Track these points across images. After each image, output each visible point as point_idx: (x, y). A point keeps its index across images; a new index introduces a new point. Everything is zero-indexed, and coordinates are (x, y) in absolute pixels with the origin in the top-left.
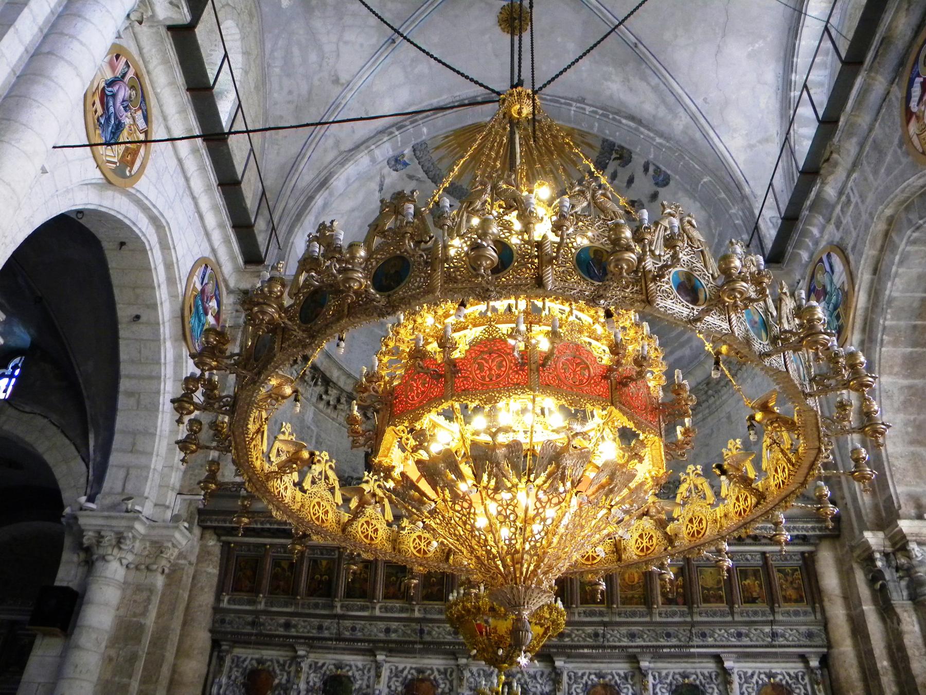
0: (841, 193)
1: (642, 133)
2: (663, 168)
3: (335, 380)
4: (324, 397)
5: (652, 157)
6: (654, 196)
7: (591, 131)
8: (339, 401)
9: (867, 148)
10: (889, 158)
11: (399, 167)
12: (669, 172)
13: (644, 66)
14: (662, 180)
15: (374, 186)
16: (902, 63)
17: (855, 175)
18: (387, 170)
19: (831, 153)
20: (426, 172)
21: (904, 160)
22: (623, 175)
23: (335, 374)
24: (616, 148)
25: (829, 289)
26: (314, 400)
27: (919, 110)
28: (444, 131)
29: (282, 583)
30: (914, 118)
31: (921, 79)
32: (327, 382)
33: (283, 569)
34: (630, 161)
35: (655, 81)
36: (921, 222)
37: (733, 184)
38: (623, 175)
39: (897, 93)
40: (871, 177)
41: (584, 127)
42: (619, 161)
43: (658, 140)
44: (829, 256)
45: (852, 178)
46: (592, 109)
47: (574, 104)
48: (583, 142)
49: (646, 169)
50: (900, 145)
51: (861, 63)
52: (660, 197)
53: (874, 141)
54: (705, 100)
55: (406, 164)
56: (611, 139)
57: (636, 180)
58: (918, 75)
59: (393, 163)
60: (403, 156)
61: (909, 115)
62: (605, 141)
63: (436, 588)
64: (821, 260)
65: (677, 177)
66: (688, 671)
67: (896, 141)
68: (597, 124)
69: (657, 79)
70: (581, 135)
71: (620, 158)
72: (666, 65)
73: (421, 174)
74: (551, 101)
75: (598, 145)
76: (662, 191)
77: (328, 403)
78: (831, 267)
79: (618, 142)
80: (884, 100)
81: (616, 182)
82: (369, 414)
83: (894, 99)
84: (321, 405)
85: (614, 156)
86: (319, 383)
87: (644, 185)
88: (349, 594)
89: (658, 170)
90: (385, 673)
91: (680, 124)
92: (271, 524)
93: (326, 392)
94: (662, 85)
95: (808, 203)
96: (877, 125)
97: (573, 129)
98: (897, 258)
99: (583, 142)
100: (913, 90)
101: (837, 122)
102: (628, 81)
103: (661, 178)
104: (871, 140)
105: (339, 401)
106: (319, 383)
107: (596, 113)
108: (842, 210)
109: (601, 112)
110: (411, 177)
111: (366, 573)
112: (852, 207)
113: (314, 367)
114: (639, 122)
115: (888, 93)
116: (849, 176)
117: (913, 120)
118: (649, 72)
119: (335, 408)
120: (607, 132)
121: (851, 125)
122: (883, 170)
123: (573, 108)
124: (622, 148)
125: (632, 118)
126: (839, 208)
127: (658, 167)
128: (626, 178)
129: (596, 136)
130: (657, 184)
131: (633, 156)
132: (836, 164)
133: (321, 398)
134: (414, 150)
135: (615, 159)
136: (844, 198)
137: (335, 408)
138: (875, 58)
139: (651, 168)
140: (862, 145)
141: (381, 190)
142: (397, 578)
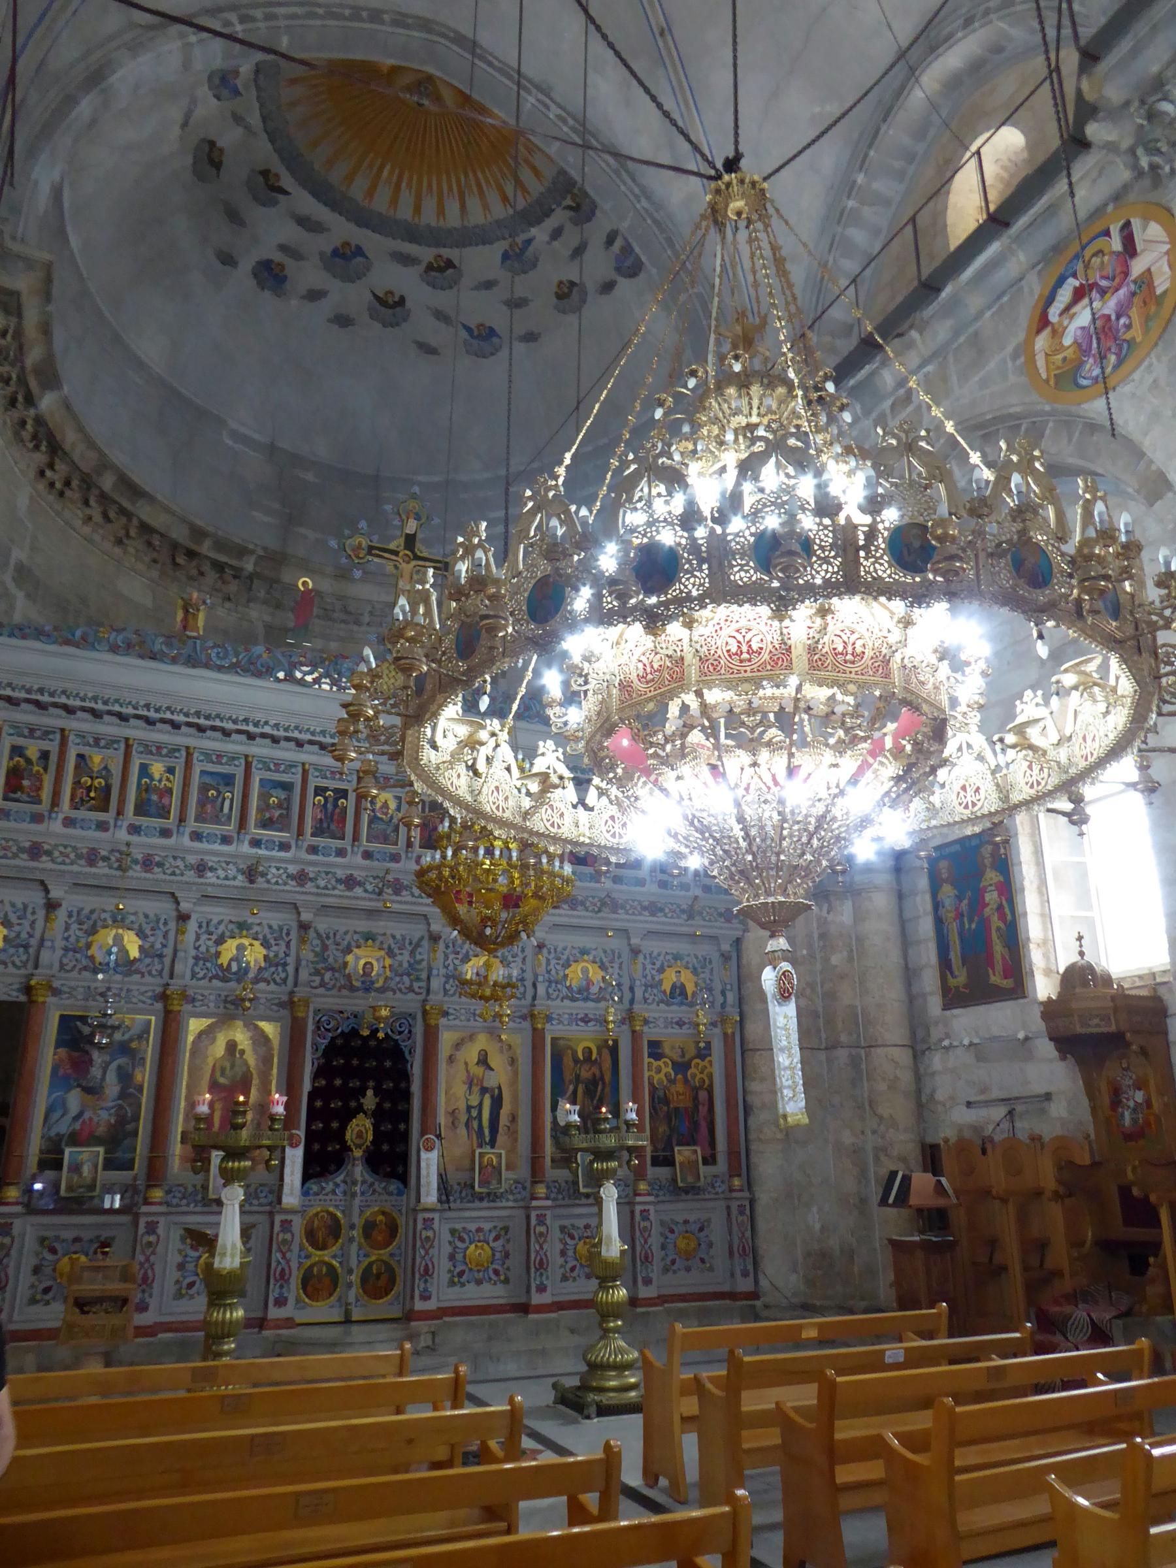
1: (625, 184)
2: (637, 249)
3: (67, 447)
4: (48, 473)
6: (608, 287)
7: (547, 150)
8: (67, 483)
9: (962, 339)
10: (992, 365)
11: (225, 93)
12: (643, 259)
14: (630, 266)
15: (175, 113)
16: (1057, 249)
17: (929, 368)
18: (204, 91)
19: (911, 327)
20: (264, 119)
21: (1012, 379)
22: (571, 237)
23: (70, 438)
24: (576, 191)
26: (32, 474)
27: (1060, 323)
29: (26, 783)
30: (1048, 330)
31: (1077, 283)
32: (55, 449)
33: (29, 761)
34: (589, 220)
38: (571, 237)
39: (1035, 287)
40: (954, 379)
42: (572, 213)
43: (644, 203)
45: (925, 370)
46: (559, 112)
47: (534, 91)
48: (526, 161)
49: (610, 240)
50: (1015, 356)
51: (1007, 225)
52: (617, 291)
53: (976, 334)
55: (237, 93)
57: (588, 255)
58: (1075, 276)
59: (217, 81)
60: (236, 73)
61: (1043, 322)
62: (562, 172)
63: (277, 813)
65: (654, 271)
66: (588, 946)
67: (1010, 349)
70: (527, 148)
71: (576, 209)
73: (255, 120)
74: (500, 70)
76: (623, 284)
77: (52, 485)
80: (1012, 286)
81: (555, 243)
82: (112, 515)
83: (1026, 290)
84: (41, 486)
85: (568, 202)
86: (43, 448)
87: (598, 264)
88: (142, 809)
89: (627, 249)
90: (192, 926)
92: (13, 690)
93: (51, 466)
95: (852, 382)
96: (988, 314)
99: (526, 161)
100: (1061, 291)
101: (938, 290)
103: (628, 263)
104: (971, 330)
105: (67, 483)
106: (43, 448)
107: (565, 122)
108: (893, 406)
109: (571, 122)
110: (238, 119)
111: (168, 779)
112: (910, 409)
113: (39, 421)
115: (1021, 279)
117: (1047, 332)
119: (61, 494)
121: (955, 300)
122: (976, 379)
123: (532, 100)
124: (586, 194)
126: (889, 402)
128: (575, 243)
130: (618, 270)
131: (598, 213)
132: (911, 345)
133: (42, 473)
134: (257, 71)
135: (569, 208)
136: (902, 391)
137: (61, 494)
138: (1031, 224)
139: (618, 243)
140: (957, 333)
141: (185, 125)
142: (219, 793)
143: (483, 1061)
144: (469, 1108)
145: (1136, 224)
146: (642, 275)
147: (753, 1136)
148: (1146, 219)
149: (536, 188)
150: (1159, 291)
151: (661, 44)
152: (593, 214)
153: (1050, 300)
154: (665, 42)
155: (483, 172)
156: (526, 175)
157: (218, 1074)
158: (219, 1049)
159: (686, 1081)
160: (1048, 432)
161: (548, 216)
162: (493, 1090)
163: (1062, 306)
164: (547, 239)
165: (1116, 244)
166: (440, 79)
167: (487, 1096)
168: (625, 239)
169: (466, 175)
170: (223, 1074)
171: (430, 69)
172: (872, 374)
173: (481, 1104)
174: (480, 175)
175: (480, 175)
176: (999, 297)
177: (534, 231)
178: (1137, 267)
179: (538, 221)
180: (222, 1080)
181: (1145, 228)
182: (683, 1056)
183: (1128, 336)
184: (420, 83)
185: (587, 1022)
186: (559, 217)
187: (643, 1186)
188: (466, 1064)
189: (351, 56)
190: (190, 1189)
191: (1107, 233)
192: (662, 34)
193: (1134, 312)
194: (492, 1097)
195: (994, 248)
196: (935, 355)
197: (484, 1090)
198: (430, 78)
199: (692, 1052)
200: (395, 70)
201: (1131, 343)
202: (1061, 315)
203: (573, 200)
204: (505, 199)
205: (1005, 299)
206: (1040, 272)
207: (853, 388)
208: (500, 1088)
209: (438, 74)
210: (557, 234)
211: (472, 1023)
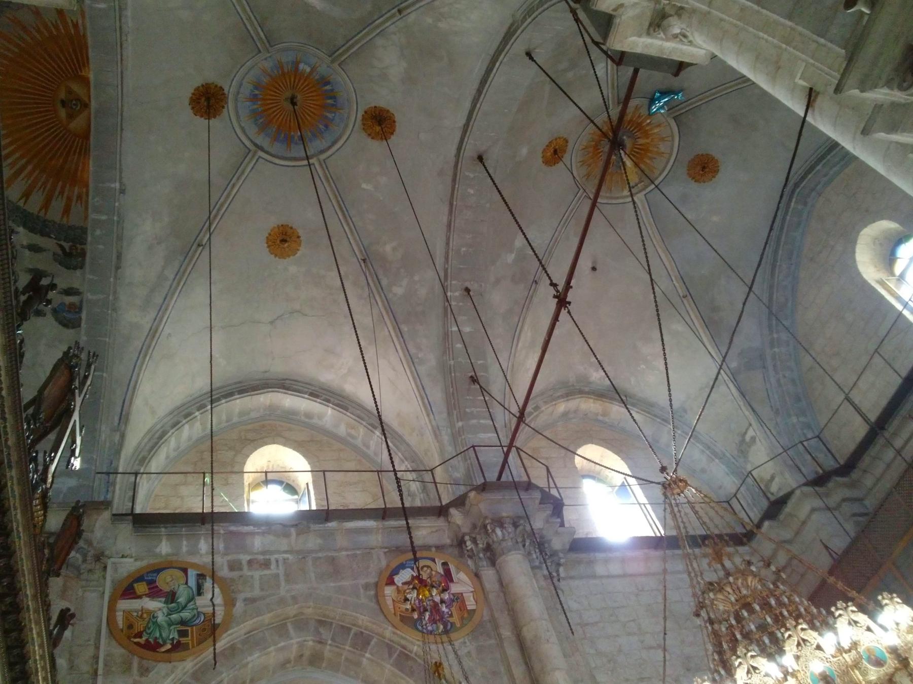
0: (263, 553)
2: (84, 315)
5: (90, 296)
7: (90, 210)
12: (83, 324)
13: (182, 258)
25: (182, 600)
28: (88, 25)
34: (68, 268)
35: (170, 274)
36: (330, 642)
37: (118, 410)
41: (94, 200)
42: (60, 252)
44: (201, 577)
45: (286, 556)
48: (69, 199)
51: (383, 518)
54: (169, 334)
56: (89, 239)
61: (391, 582)
62: (84, 231)
64: (185, 571)
68: (104, 217)
69: (172, 277)
70: (79, 197)
71: (67, 255)
72: (188, 282)
75: (74, 219)
78: (200, 588)
79: (88, 248)
83: (375, 556)
85: (67, 246)
89: (77, 309)
91: (133, 316)
94: (169, 283)
97: (87, 186)
98: (283, 644)
99: (69, 199)
102: (159, 243)
112: (267, 572)
114: (118, 268)
116: (286, 552)
118: (176, 264)
120: (98, 232)
124: (83, 254)
125: (119, 257)
126: (248, 558)
127: (80, 309)
129: (86, 217)
131: (78, 272)
135: (61, 247)
145: (452, 567)
146: (71, 332)
148: (458, 570)
149: (55, 214)
150: (469, 608)
151: (194, 247)
152: (75, 268)
153: (396, 572)
154: (196, 251)
155: (33, 170)
156: (58, 205)
160: (373, 643)
161: (42, 235)
163: (404, 581)
164: (25, 243)
165: (440, 570)
166: (90, 114)
168: (81, 302)
169: (22, 157)
171: (93, 104)
172: (253, 534)
174: (30, 168)
175: (30, 168)
176: (359, 549)
177: (21, 229)
178: (455, 588)
179: (32, 230)
181: (457, 573)
183: (451, 620)
184: (78, 99)
186: (49, 244)
189: (90, 50)
191: (434, 560)
192: (199, 245)
193: (453, 609)
195: (370, 523)
196: (298, 552)
198: (86, 106)
200: (86, 82)
201: (452, 624)
202: (404, 584)
203: (71, 248)
204: (27, 195)
205: (358, 552)
206: (385, 553)
207: (231, 532)
209: (93, 111)
210: (34, 248)
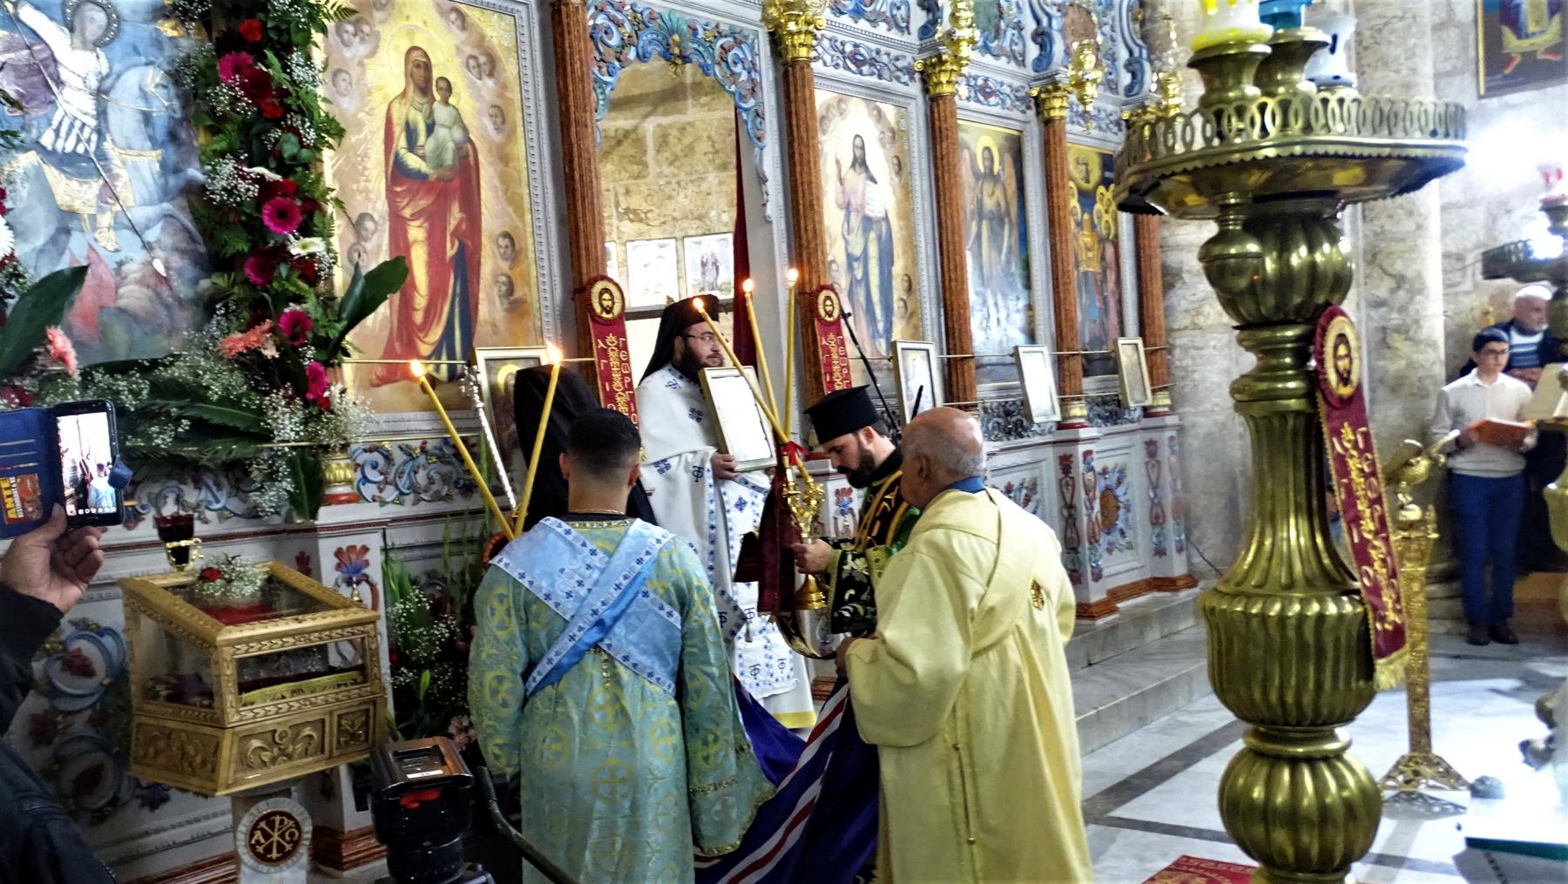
143: (860, 163)
144: (851, 259)
147: (1181, 321)
157: (401, 142)
158: (385, 74)
159: (1093, 227)
162: (879, 221)
167: (872, 235)
170: (412, 146)
173: (865, 251)
180: (413, 161)
182: (1088, 181)
185: (987, 95)
187: (1078, 411)
188: (838, 162)
190: (399, 457)
194: (879, 237)
197: (868, 222)
199: (1096, 175)
208: (886, 219)
211: (842, 73)
